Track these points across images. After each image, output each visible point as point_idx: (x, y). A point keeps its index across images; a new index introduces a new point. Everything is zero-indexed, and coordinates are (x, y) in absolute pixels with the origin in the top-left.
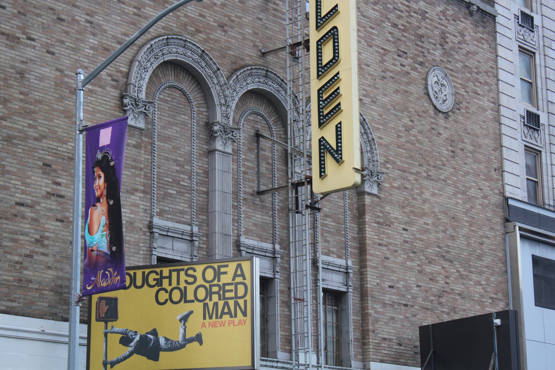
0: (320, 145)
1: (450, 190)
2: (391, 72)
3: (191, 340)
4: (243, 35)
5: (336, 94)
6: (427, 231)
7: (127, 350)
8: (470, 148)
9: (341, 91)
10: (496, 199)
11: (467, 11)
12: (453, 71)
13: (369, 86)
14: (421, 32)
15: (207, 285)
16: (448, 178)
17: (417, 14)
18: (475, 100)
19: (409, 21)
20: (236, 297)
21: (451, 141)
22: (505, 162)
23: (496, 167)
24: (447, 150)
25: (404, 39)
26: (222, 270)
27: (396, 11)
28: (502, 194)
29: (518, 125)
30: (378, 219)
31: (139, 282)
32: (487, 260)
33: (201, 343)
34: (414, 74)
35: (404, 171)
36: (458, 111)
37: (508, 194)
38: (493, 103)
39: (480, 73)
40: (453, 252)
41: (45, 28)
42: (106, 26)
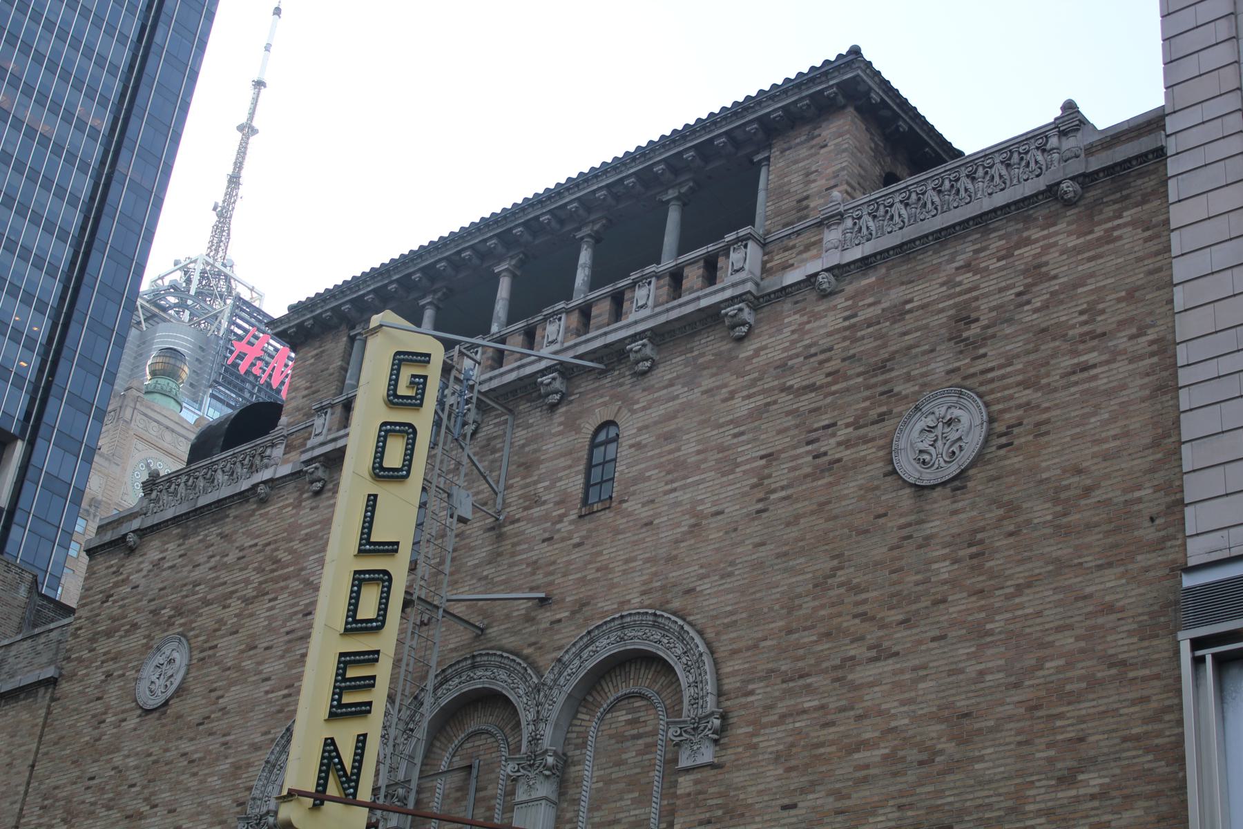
2: (783, 488)
11: (1055, 207)
12: (992, 369)
13: (717, 550)
14: (884, 354)
16: (953, 624)
17: (879, 323)
18: (1073, 390)
19: (852, 352)
23: (1154, 510)
24: (955, 562)
25: (829, 399)
27: (812, 360)
30: (708, 815)
34: (846, 454)
35: (801, 677)
36: (1002, 452)
38: (1152, 354)
39: (1103, 312)
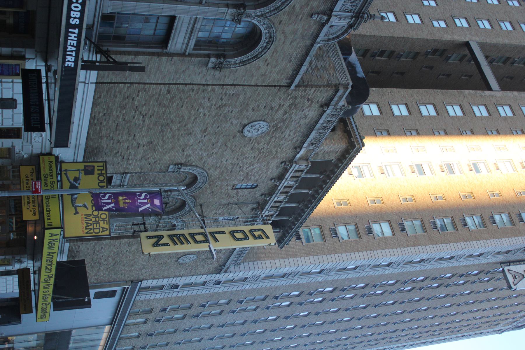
0: (161, 236)
1: (145, 263)
3: (76, 209)
4: (209, 198)
5: (182, 243)
6: (126, 257)
7: (72, 180)
8: (163, 269)
9: (183, 245)
10: (141, 278)
15: (99, 216)
20: (94, 229)
21: (166, 263)
22: (157, 280)
26: (105, 222)
28: (144, 279)
29: (173, 282)
31: (101, 184)
32: (115, 276)
33: (75, 214)
37: (143, 281)
40: (118, 266)
41: (210, 140)
42: (211, 158)
